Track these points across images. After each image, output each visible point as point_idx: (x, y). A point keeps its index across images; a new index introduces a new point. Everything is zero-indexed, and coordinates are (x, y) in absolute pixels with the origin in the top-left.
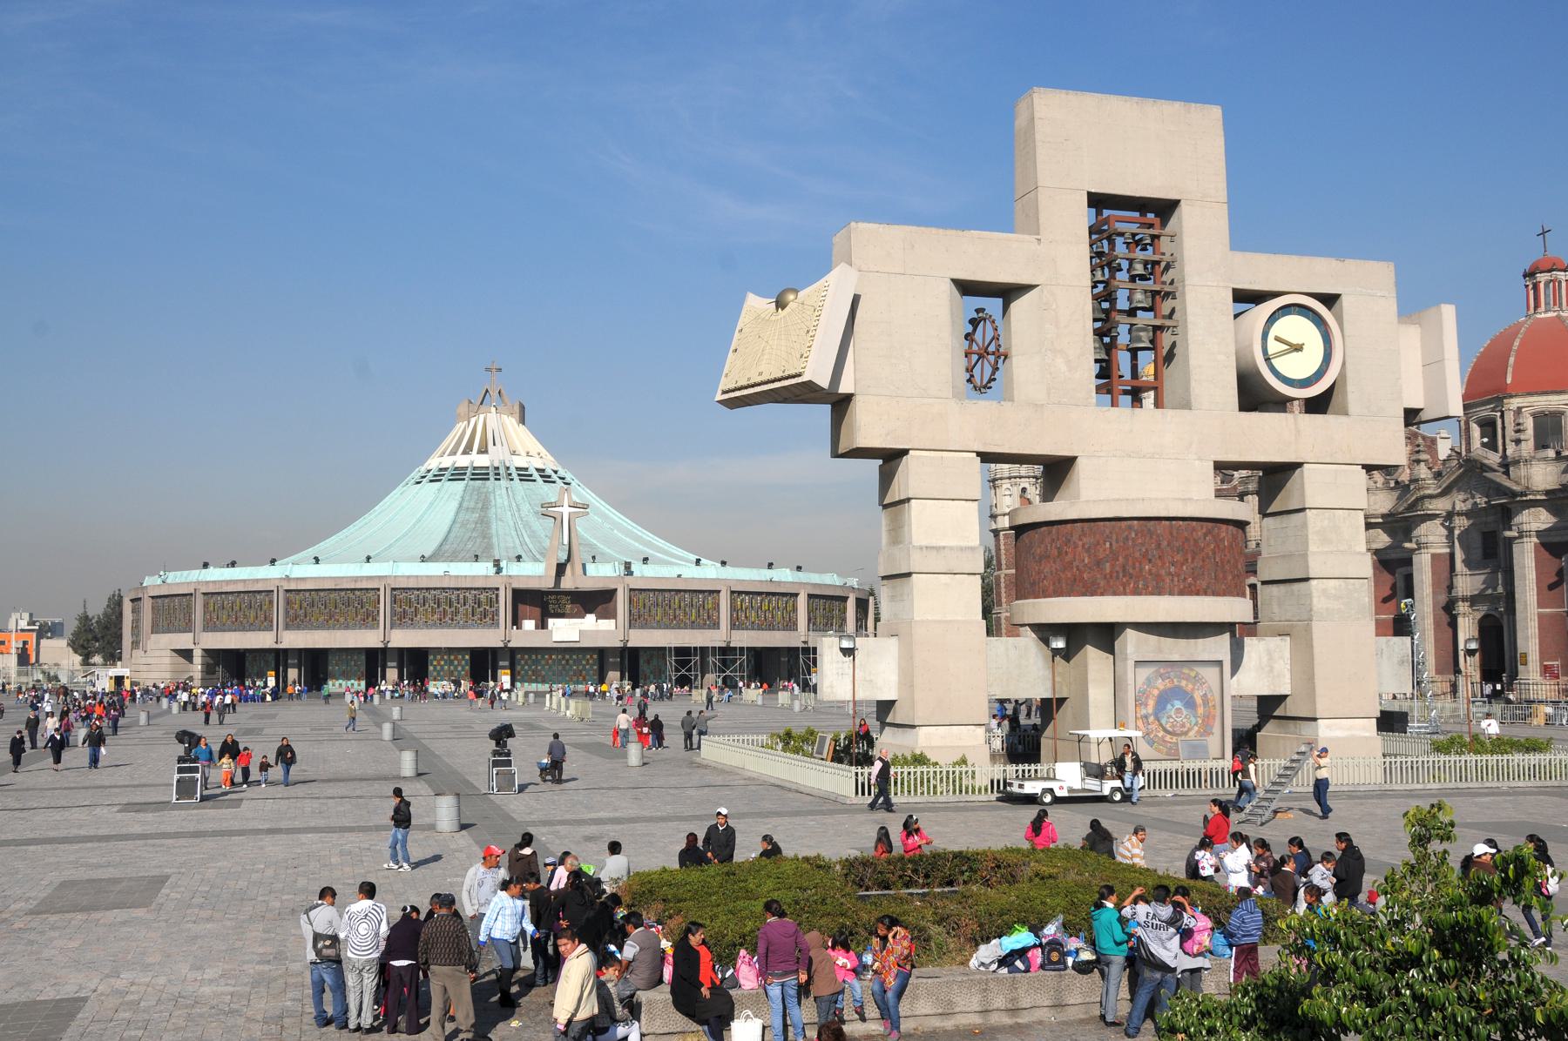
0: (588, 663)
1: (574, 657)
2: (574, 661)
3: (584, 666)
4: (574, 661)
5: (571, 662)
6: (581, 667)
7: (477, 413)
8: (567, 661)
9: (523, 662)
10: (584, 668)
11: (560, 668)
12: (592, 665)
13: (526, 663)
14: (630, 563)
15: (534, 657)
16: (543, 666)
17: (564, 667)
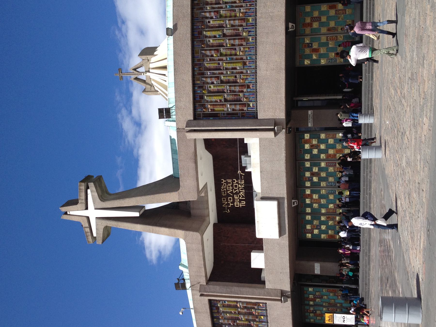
0: (317, 147)
1: (308, 165)
2: (313, 165)
3: (321, 151)
4: (313, 165)
5: (315, 170)
6: (323, 156)
7: (152, 85)
8: (313, 174)
9: (316, 232)
10: (325, 151)
11: (323, 184)
12: (321, 141)
13: (318, 227)
14: (161, 111)
15: (308, 217)
16: (321, 206)
17: (321, 179)
